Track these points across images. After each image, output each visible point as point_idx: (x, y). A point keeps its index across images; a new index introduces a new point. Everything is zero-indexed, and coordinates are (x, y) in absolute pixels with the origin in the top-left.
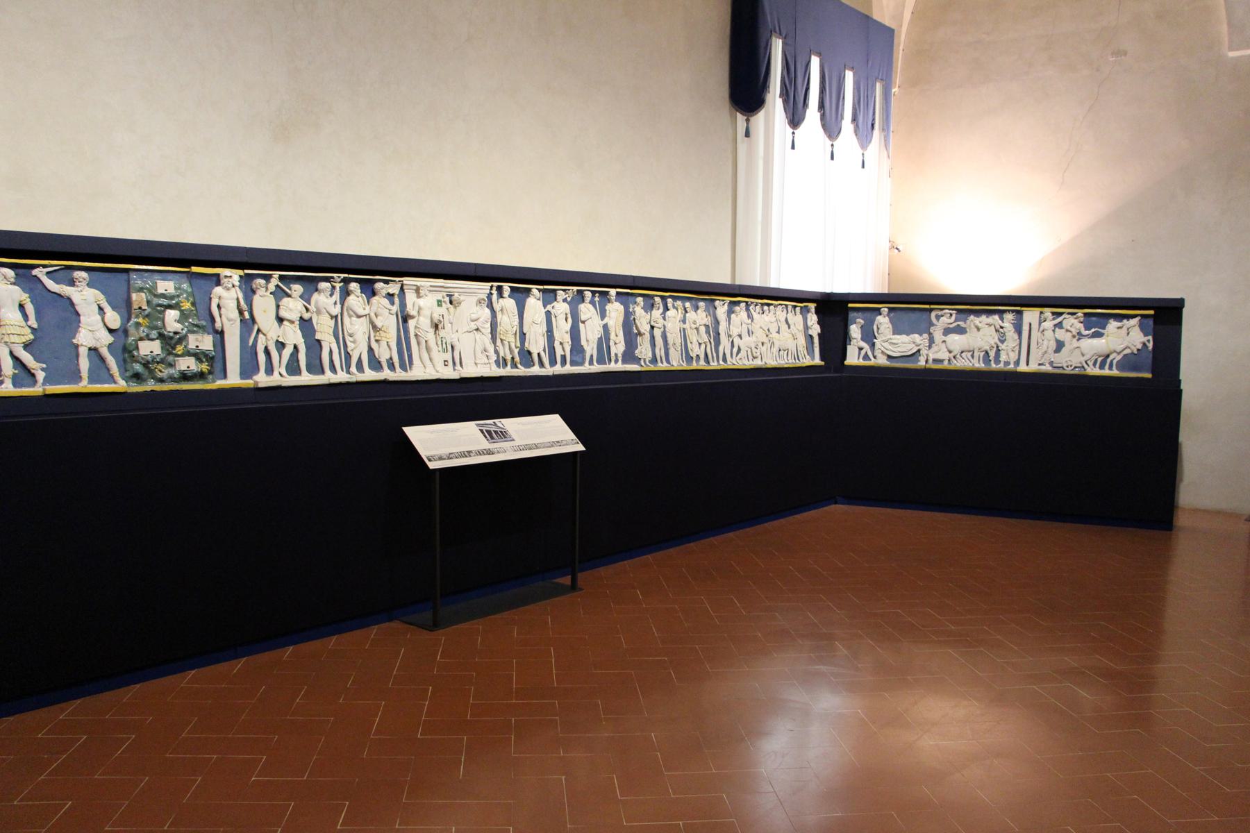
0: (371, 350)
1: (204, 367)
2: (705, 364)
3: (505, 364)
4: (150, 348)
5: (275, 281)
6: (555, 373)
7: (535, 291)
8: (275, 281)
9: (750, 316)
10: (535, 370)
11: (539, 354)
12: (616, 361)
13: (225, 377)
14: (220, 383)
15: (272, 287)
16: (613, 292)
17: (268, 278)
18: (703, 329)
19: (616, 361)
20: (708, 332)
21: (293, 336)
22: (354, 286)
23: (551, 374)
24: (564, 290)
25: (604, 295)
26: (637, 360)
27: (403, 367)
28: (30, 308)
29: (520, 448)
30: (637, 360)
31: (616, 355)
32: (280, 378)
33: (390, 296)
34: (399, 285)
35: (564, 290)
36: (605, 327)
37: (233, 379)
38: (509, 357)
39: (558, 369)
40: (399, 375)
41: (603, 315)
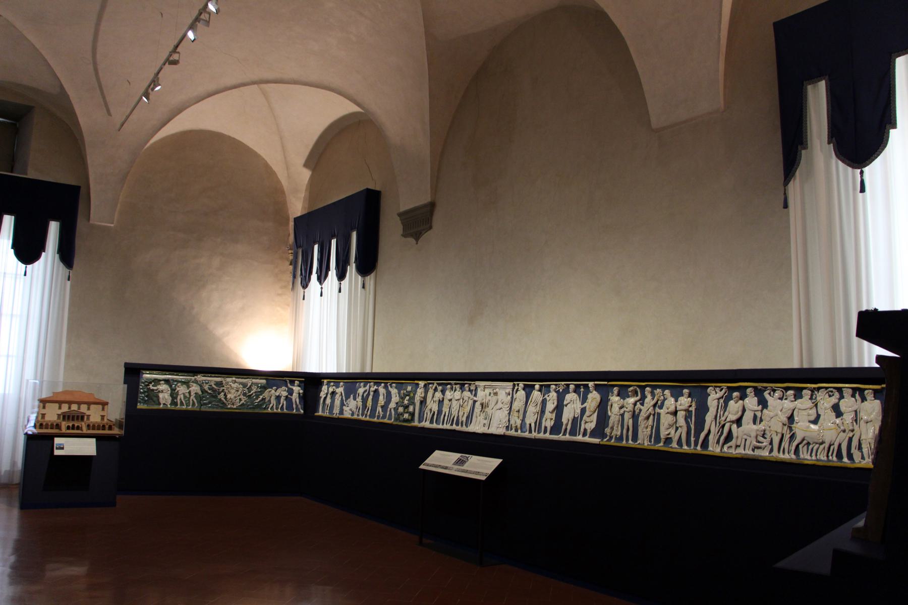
0: (458, 416)
1: (410, 418)
2: (677, 446)
3: (511, 429)
4: (401, 410)
5: (435, 385)
6: (536, 438)
7: (537, 387)
8: (435, 385)
9: (763, 403)
10: (526, 434)
11: (530, 425)
12: (545, 432)
13: (414, 422)
14: (413, 424)
15: (434, 388)
16: (591, 384)
17: (433, 384)
18: (681, 415)
19: (545, 432)
20: (687, 418)
21: (435, 408)
22: (458, 387)
23: (534, 438)
24: (556, 385)
25: (861, 391)
26: (603, 436)
27: (467, 426)
28: (385, 395)
29: (463, 471)
30: (603, 436)
31: (546, 428)
32: (427, 424)
33: (470, 390)
34: (474, 386)
35: (556, 385)
36: (583, 411)
37: (416, 423)
38: (513, 425)
39: (541, 436)
40: (464, 429)
41: (584, 400)
